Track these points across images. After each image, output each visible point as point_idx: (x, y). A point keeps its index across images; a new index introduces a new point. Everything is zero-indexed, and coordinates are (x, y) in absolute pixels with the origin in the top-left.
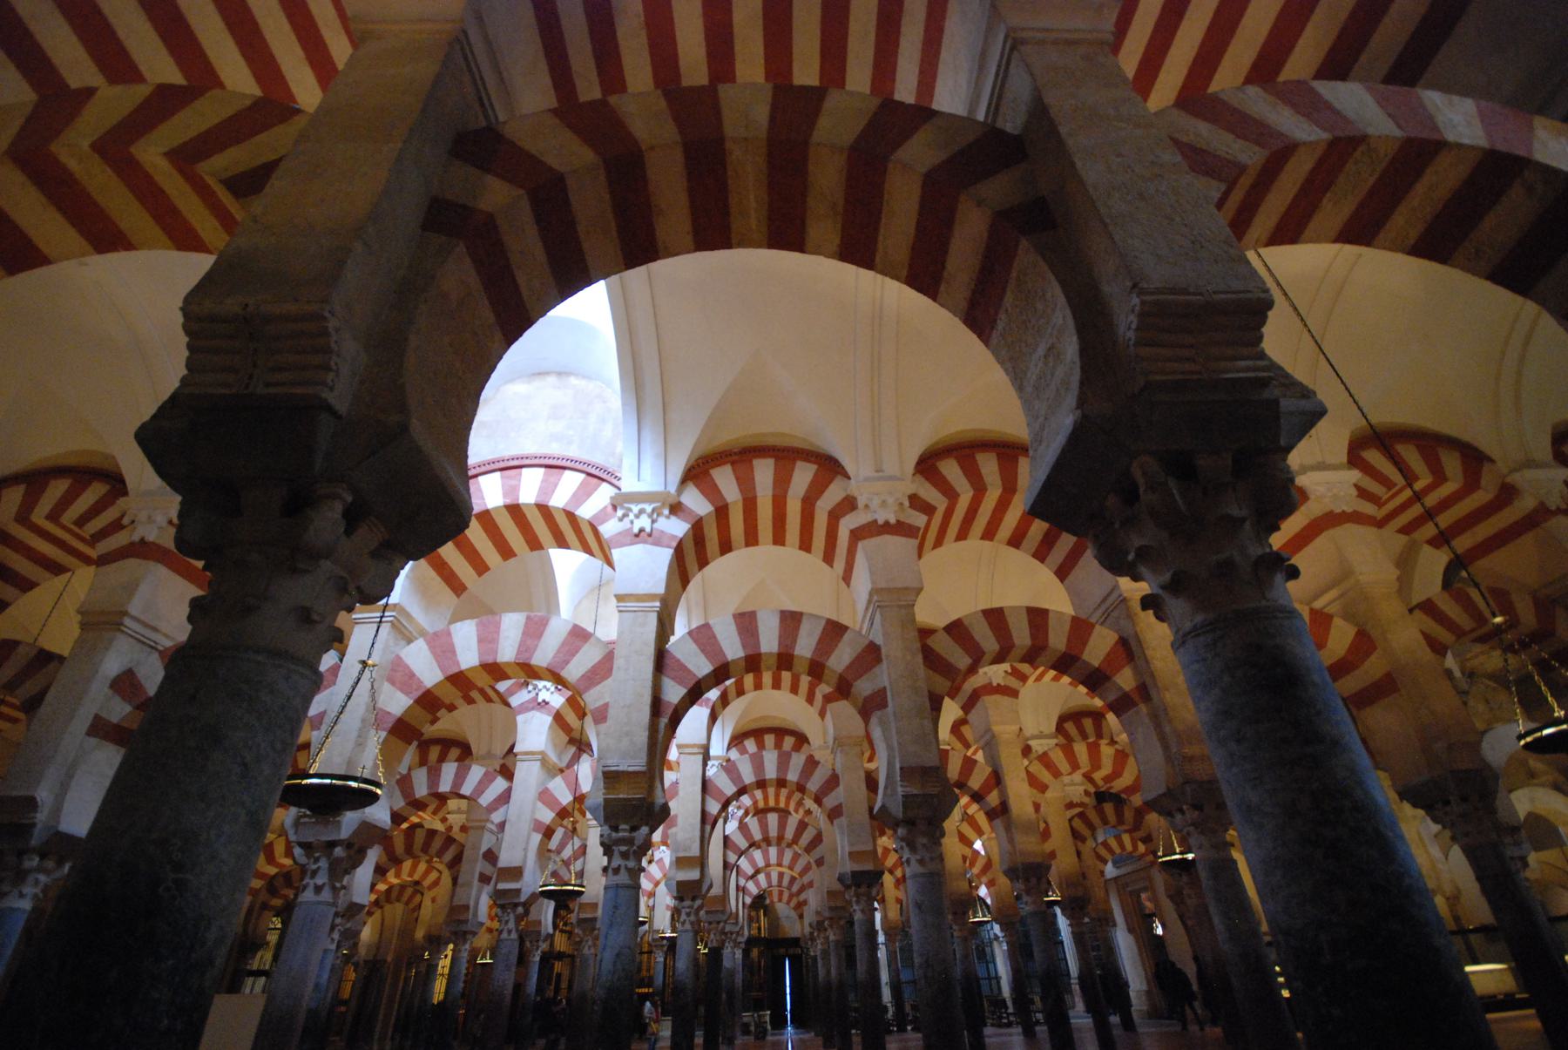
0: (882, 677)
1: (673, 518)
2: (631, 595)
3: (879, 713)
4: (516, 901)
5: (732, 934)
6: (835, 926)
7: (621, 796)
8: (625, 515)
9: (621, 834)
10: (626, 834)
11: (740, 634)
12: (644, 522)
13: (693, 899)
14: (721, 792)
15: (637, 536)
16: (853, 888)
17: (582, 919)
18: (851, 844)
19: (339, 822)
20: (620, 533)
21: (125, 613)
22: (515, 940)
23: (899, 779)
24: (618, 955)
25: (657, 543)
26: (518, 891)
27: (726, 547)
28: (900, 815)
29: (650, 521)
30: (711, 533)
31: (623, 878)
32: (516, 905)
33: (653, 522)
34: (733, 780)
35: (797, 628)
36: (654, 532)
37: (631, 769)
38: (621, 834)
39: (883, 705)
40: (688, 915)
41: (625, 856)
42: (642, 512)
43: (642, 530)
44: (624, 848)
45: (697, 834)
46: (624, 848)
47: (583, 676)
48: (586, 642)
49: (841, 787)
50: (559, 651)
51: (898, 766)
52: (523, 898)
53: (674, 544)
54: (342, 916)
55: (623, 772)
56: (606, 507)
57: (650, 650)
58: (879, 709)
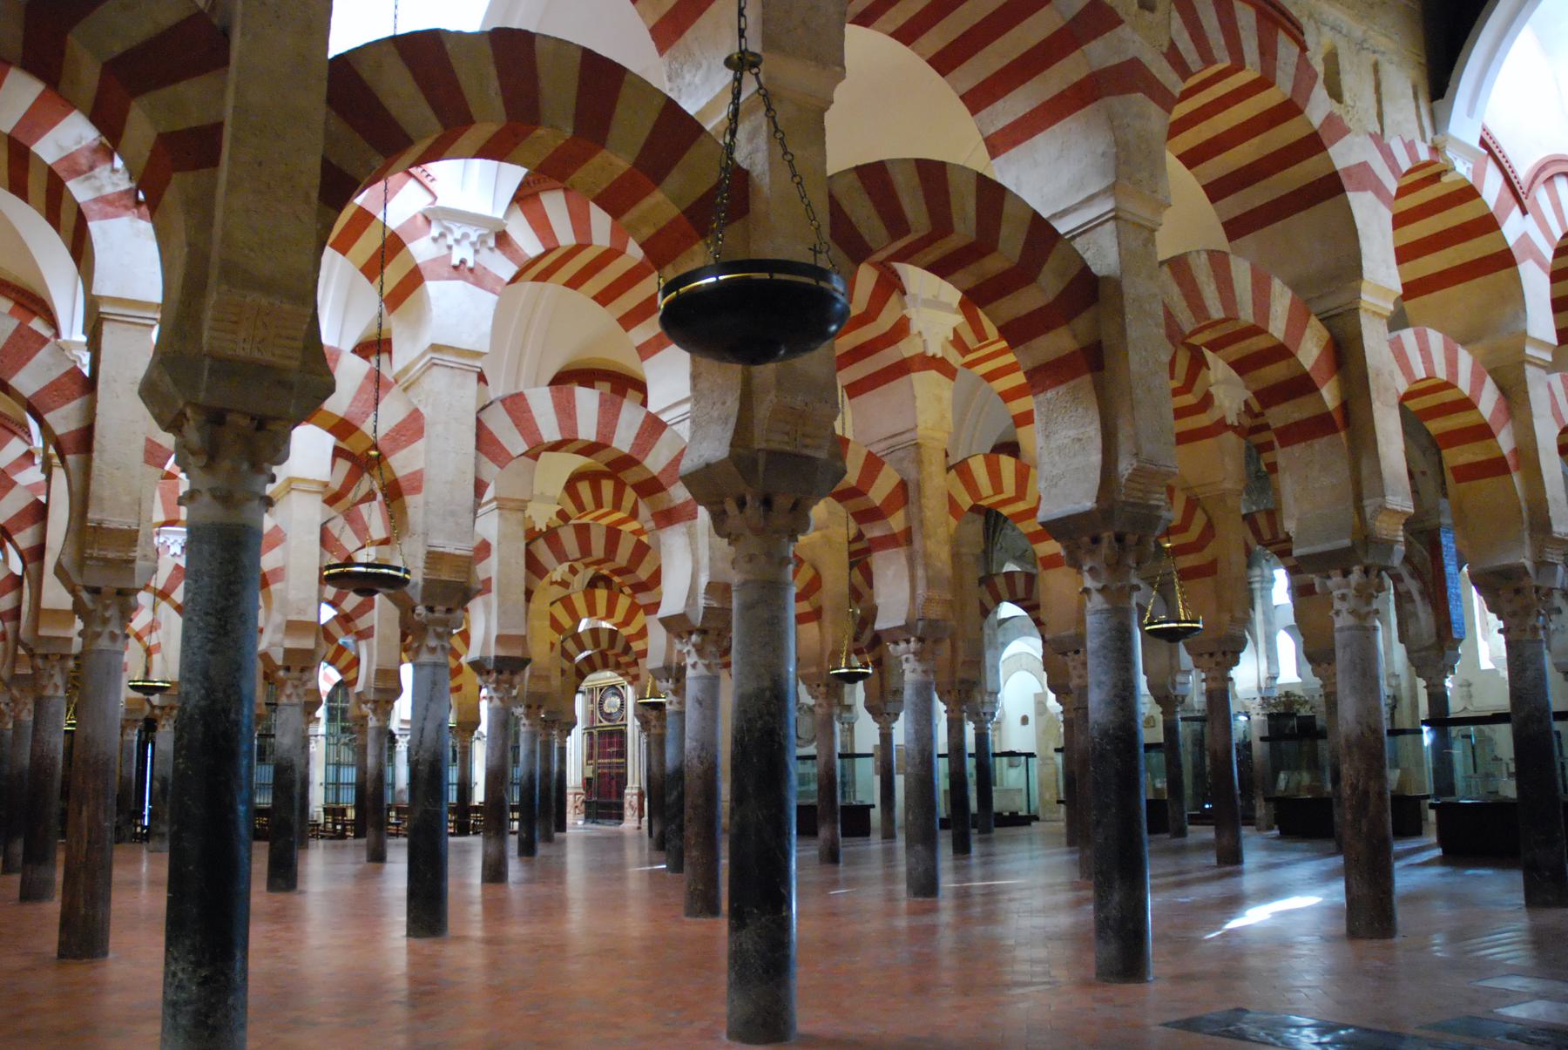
1: (498, 252)
2: (452, 348)
6: (379, 711)
8: (442, 235)
9: (437, 615)
12: (462, 253)
15: (455, 267)
18: (500, 625)
19: (133, 569)
22: (62, 698)
25: (479, 283)
32: (64, 657)
33: (476, 252)
37: (458, 552)
38: (437, 615)
40: (296, 687)
41: (439, 636)
42: (465, 236)
43: (463, 262)
44: (440, 629)
47: (387, 434)
50: (355, 399)
55: (449, 554)
56: (415, 216)
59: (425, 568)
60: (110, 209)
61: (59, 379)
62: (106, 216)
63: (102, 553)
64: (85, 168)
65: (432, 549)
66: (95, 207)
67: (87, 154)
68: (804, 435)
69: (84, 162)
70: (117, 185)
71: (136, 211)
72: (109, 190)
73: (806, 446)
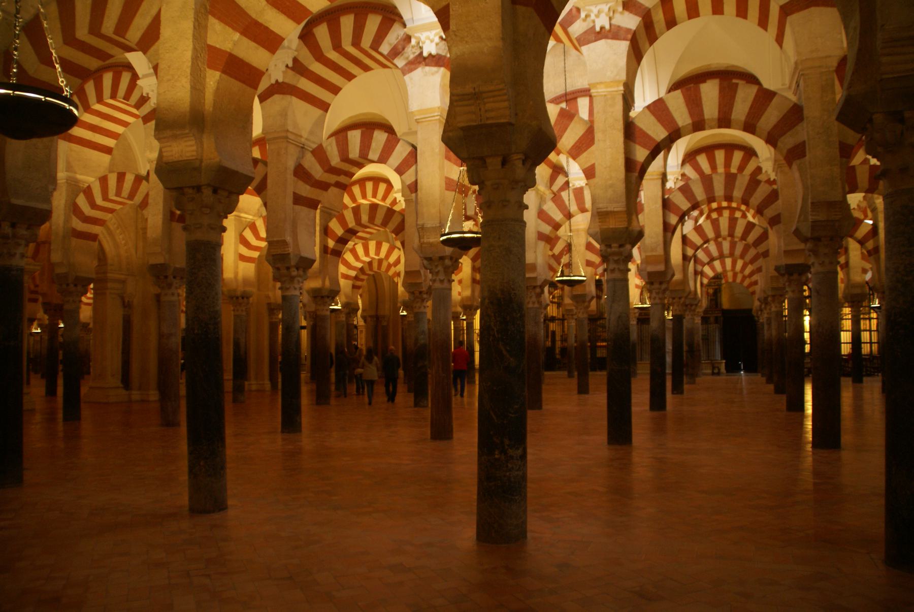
0: (802, 133)
1: (626, 13)
3: (798, 162)
4: (535, 284)
5: (692, 305)
7: (611, 227)
8: (587, 16)
9: (613, 250)
10: (617, 250)
11: (687, 105)
12: (602, 22)
13: (661, 283)
14: (678, 208)
15: (599, 33)
16: (786, 276)
17: (574, 295)
20: (585, 32)
21: (288, 131)
23: (810, 210)
24: (619, 317)
26: (535, 279)
27: (671, 23)
28: (809, 235)
29: (608, 19)
30: (659, 18)
31: (617, 275)
32: (535, 287)
33: (610, 19)
34: (687, 198)
35: (733, 98)
36: (613, 27)
37: (615, 210)
38: (613, 250)
39: (802, 154)
40: (658, 293)
41: (617, 262)
42: (599, 12)
43: (602, 28)
44: (616, 258)
45: (661, 238)
46: (616, 258)
48: (571, 121)
49: (780, 202)
51: (810, 201)
52: (539, 283)
53: (630, 36)
54: (427, 293)
57: (620, 125)
58: (798, 158)
59: (599, 222)
60: (413, 66)
61: (406, 157)
62: (411, 71)
63: (428, 240)
64: (401, 50)
65: (599, 210)
66: (406, 68)
67: (402, 42)
68: (486, 111)
69: (400, 47)
70: (415, 53)
71: (424, 63)
72: (412, 57)
73: (487, 119)
